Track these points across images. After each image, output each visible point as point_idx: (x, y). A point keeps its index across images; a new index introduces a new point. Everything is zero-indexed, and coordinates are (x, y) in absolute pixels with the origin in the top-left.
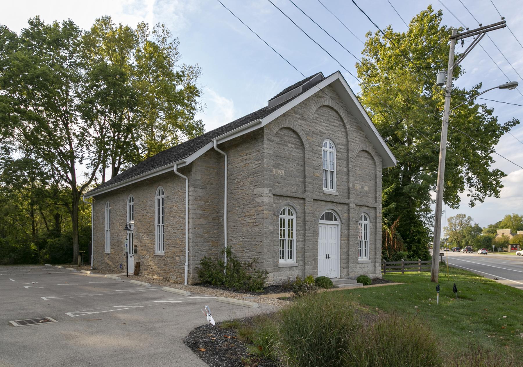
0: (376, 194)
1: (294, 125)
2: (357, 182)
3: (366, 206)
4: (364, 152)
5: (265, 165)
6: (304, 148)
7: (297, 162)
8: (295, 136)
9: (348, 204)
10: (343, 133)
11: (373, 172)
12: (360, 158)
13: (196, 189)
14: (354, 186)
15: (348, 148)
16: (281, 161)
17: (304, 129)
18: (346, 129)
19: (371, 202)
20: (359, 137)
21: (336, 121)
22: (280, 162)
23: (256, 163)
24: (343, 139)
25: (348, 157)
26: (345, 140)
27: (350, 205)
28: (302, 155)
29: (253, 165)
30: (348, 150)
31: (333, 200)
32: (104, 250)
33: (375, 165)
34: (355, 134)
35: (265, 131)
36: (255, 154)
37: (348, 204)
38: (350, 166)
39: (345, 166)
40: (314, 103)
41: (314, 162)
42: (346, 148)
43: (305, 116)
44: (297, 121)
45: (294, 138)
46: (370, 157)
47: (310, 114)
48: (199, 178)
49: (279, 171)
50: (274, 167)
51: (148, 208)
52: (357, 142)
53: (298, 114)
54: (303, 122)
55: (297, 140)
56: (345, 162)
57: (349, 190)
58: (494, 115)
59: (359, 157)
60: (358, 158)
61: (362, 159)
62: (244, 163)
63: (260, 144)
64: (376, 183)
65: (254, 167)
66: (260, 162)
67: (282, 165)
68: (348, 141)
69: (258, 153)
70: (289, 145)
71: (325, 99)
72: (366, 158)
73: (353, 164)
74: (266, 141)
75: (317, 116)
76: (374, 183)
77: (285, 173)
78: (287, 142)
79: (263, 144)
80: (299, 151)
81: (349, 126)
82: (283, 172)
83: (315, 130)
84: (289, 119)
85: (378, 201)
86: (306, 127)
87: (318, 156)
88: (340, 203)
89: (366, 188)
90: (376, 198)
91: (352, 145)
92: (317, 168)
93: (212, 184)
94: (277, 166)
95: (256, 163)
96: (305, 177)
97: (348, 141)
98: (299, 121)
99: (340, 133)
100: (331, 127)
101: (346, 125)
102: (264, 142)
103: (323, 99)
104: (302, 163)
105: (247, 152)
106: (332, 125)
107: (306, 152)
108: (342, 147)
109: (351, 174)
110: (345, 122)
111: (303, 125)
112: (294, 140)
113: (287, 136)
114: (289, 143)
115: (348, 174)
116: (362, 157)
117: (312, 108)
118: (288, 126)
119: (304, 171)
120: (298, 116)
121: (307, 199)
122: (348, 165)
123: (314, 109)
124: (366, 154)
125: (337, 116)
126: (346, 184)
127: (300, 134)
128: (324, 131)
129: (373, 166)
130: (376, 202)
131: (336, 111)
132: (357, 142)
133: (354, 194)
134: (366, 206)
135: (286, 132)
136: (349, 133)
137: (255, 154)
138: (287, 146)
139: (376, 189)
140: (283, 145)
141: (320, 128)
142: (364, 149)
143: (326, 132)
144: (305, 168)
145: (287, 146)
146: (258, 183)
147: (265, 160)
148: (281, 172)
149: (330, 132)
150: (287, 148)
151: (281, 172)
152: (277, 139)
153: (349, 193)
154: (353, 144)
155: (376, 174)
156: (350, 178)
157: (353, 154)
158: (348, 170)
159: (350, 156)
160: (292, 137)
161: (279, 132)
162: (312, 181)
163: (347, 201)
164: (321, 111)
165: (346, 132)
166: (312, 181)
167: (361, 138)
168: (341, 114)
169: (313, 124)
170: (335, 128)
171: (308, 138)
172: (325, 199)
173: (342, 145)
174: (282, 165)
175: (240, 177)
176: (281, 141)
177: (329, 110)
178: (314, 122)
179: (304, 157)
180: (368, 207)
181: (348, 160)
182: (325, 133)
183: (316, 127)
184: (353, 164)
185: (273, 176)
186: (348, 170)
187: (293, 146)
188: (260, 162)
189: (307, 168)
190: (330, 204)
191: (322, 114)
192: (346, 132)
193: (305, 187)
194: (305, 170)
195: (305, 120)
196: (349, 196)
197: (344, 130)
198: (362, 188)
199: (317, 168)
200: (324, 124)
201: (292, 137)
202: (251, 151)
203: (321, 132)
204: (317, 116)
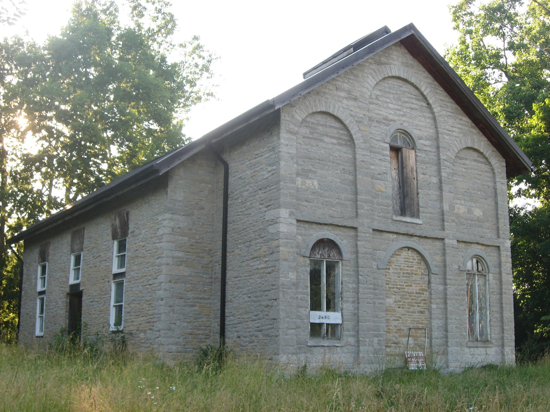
0: (498, 222)
1: (334, 107)
2: (459, 202)
3: (478, 243)
4: (471, 152)
5: (282, 172)
6: (354, 143)
7: (342, 167)
8: (337, 125)
9: (443, 239)
10: (428, 120)
11: (491, 184)
12: (463, 161)
13: (175, 216)
14: (452, 207)
15: (438, 144)
16: (313, 166)
17: (352, 113)
18: (433, 113)
19: (489, 236)
20: (460, 126)
21: (414, 101)
22: (310, 167)
23: (270, 169)
24: (428, 130)
25: (439, 159)
26: (432, 131)
27: (447, 241)
28: (351, 156)
29: (264, 173)
30: (438, 148)
31: (411, 231)
32: (34, 332)
33: (494, 173)
34: (451, 121)
35: (282, 117)
36: (267, 155)
37: (443, 239)
38: (443, 174)
39: (435, 174)
40: (371, 74)
41: (372, 167)
42: (435, 144)
43: (355, 94)
44: (341, 102)
45: (336, 128)
46: (481, 160)
47: (365, 90)
48: (180, 199)
49: (308, 182)
50: (298, 174)
51: (102, 254)
52: (454, 134)
53: (343, 90)
54: (351, 103)
55: (342, 132)
56: (434, 168)
57: (443, 214)
58: (454, 24)
59: (461, 159)
60: (459, 161)
61: (467, 162)
62: (252, 171)
63: (275, 138)
64: (496, 203)
65: (266, 176)
66: (274, 167)
67: (315, 172)
68: (437, 132)
69: (272, 153)
70: (326, 139)
71: (392, 66)
72: (475, 160)
73: (448, 170)
74: (284, 134)
75: (378, 93)
76: (493, 203)
77: (319, 184)
78: (323, 135)
79: (279, 139)
80: (344, 149)
81: (439, 108)
82: (316, 183)
83: (375, 116)
84: (326, 98)
85: (501, 235)
86: (358, 110)
87: (382, 157)
88: (426, 237)
89: (478, 213)
90: (498, 229)
91: (445, 139)
92: (379, 176)
93: (202, 208)
94: (304, 174)
95: (270, 169)
96: (356, 193)
97: (437, 132)
98: (345, 101)
99: (423, 119)
100: (405, 110)
101: (433, 106)
102: (281, 134)
103: (387, 66)
104: (352, 168)
105: (256, 153)
106: (407, 108)
107: (359, 151)
108: (427, 143)
109: (445, 187)
110: (431, 102)
111: (352, 108)
112: (335, 131)
113: (322, 125)
114: (327, 136)
115: (441, 189)
116: (466, 159)
117: (369, 81)
118: (323, 109)
119: (355, 183)
120: (343, 94)
121: (360, 229)
122: (439, 172)
123: (373, 82)
124: (475, 154)
125: (416, 92)
126: (437, 204)
127: (347, 122)
128: (391, 117)
129: (490, 175)
130: (499, 237)
131: (412, 84)
132: (454, 134)
133: (453, 221)
134: (478, 243)
135: (320, 119)
136: (440, 120)
137: (267, 155)
138: (322, 141)
139: (497, 214)
140: (316, 139)
141: (384, 113)
142: (470, 145)
143: (395, 118)
144: (355, 176)
145: (322, 141)
146: (273, 202)
147: (282, 163)
148: (313, 184)
149: (404, 119)
150: (324, 145)
151: (313, 184)
152: (305, 131)
153: (443, 220)
154: (447, 137)
155: (495, 189)
156: (444, 193)
157: (449, 154)
158: (440, 181)
159: (442, 157)
160: (331, 127)
161: (308, 119)
162: (370, 198)
163: (440, 235)
164: (386, 85)
165: (434, 119)
166: (370, 198)
167: (464, 127)
168: (423, 89)
169: (372, 106)
170: (413, 112)
171: (362, 128)
172: (393, 228)
173: (427, 139)
174: (315, 172)
175: (246, 194)
176: (312, 133)
177: (400, 83)
178: (372, 103)
179: (355, 159)
180: (482, 245)
181: (439, 164)
182: (395, 121)
183: (377, 111)
184: (448, 170)
185: (298, 190)
186: (440, 181)
187: (334, 141)
188: (274, 167)
189: (359, 177)
190: (406, 238)
191: (387, 90)
192: (434, 119)
193: (357, 209)
194: (356, 180)
195: (355, 99)
196: (443, 226)
197: (430, 115)
198: (470, 211)
199: (379, 176)
200: (391, 106)
201: (331, 127)
202: (262, 150)
203: (386, 119)
204: (378, 93)
